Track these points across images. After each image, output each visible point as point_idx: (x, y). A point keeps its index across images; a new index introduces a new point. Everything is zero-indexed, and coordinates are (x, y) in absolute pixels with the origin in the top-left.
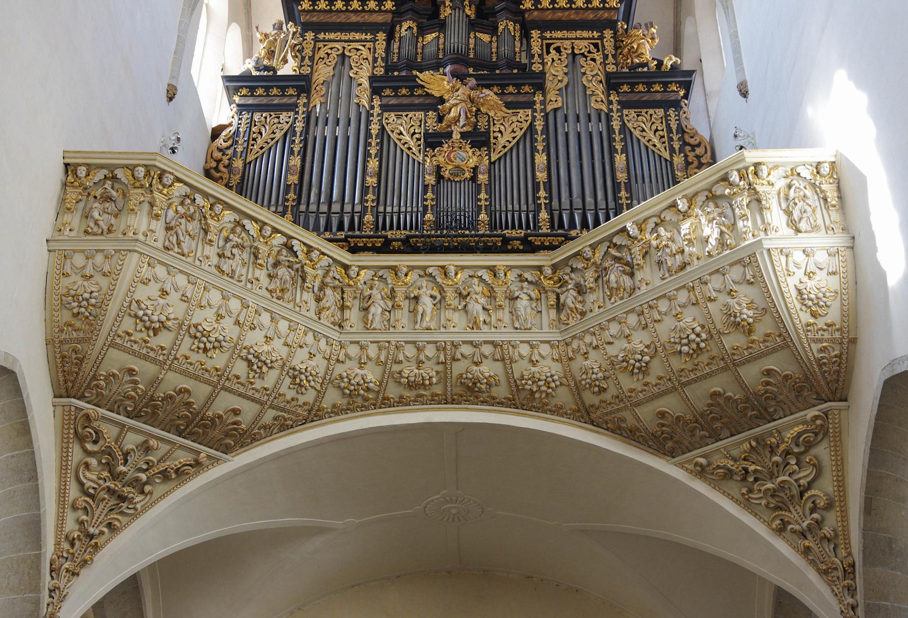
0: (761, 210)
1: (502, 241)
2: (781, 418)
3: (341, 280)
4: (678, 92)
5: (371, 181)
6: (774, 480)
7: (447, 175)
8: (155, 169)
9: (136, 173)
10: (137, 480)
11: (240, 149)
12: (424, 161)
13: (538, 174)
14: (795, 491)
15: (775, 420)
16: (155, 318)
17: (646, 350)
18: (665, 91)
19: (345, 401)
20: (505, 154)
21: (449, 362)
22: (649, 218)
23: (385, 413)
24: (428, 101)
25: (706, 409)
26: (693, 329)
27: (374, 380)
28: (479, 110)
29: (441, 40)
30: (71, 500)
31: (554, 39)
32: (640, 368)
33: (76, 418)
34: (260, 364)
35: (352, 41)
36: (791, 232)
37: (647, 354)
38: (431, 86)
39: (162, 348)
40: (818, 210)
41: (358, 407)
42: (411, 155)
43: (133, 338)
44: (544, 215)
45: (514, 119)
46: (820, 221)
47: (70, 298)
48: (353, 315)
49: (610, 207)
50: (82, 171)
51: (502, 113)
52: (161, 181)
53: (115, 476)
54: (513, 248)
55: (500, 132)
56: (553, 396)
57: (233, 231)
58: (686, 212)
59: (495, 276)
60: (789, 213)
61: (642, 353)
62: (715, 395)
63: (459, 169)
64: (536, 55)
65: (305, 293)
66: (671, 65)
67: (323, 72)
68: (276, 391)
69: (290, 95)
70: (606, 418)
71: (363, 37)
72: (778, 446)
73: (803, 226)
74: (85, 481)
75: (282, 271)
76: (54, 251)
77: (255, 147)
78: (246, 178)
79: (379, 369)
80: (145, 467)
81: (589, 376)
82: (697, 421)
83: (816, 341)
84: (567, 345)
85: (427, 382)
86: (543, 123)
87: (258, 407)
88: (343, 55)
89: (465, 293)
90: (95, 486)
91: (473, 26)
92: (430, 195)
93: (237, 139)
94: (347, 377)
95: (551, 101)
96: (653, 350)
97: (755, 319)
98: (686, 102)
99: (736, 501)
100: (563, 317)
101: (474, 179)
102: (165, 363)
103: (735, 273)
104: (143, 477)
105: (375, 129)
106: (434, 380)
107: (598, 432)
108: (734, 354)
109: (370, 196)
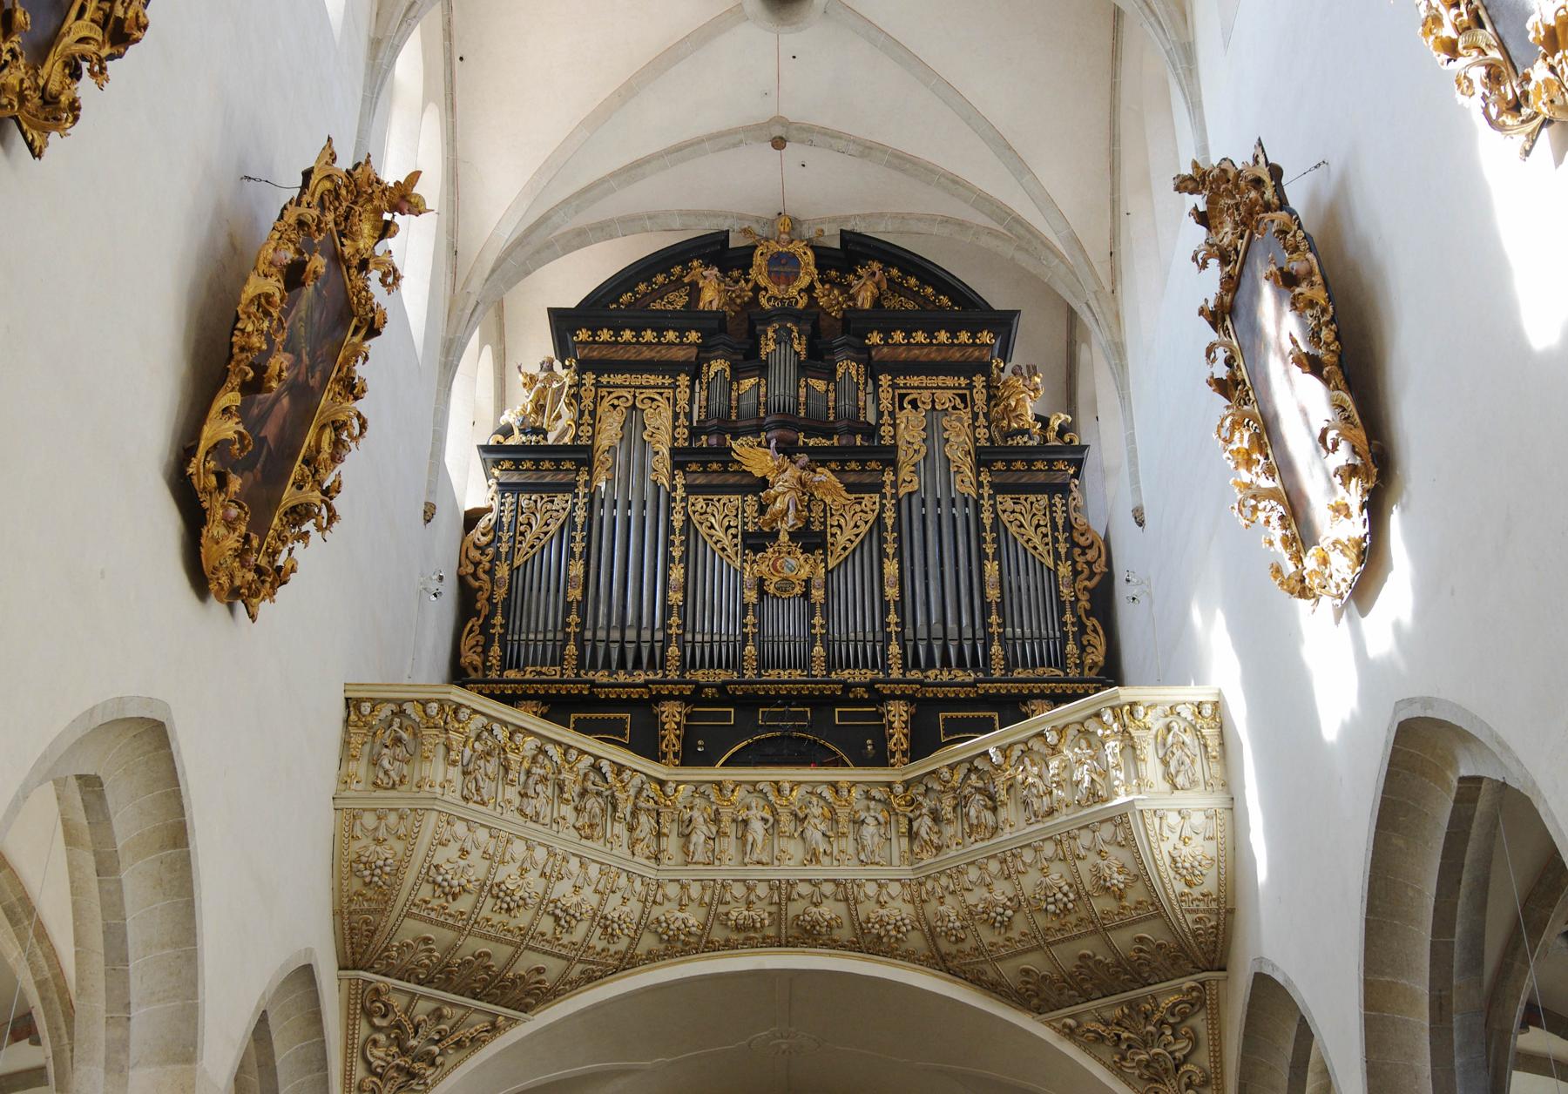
0: (1136, 759)
1: (842, 689)
2: (1156, 983)
3: (656, 798)
4: (1066, 470)
5: (676, 597)
6: (1148, 1049)
7: (771, 590)
8: (450, 703)
9: (429, 711)
10: (429, 1053)
11: (504, 549)
12: (743, 568)
13: (887, 589)
14: (1171, 1065)
15: (1150, 984)
16: (455, 882)
17: (1008, 903)
18: (1050, 470)
19: (662, 946)
20: (846, 558)
21: (783, 902)
22: (1015, 743)
23: (708, 958)
24: (745, 481)
25: (1074, 970)
26: (1060, 888)
27: (696, 924)
28: (812, 495)
29: (763, 390)
30: (357, 1082)
31: (909, 388)
32: (1002, 923)
33: (363, 992)
34: (568, 918)
35: (645, 387)
36: (1167, 786)
37: (1009, 908)
38: (751, 463)
39: (462, 913)
40: (1198, 758)
41: (677, 952)
42: (725, 558)
43: (429, 906)
44: (894, 649)
45: (858, 508)
46: (1199, 775)
47: (362, 866)
48: (672, 844)
49: (977, 637)
50: (366, 708)
51: (842, 499)
52: (456, 716)
53: (404, 1051)
54: (856, 696)
55: (839, 526)
56: (903, 941)
57: (534, 760)
58: (1056, 745)
59: (837, 792)
60: (1165, 763)
61: (1005, 907)
62: (1083, 957)
63: (786, 584)
64: (886, 412)
65: (616, 824)
66: (1060, 425)
67: (610, 431)
68: (585, 944)
69: (566, 470)
70: (964, 968)
71: (660, 381)
72: (1153, 1013)
73: (1180, 780)
74: (372, 1059)
75: (593, 804)
76: (342, 809)
77: (524, 545)
78: (514, 590)
79: (703, 911)
80: (437, 1037)
81: (945, 923)
82: (1065, 981)
83: (1191, 911)
84: (920, 884)
85: (758, 925)
86: (894, 515)
87: (565, 963)
88: (634, 407)
89: (801, 815)
90: (383, 1064)
91: (803, 369)
92: (750, 619)
93: (500, 533)
94: (665, 921)
95: (904, 481)
96: (1017, 903)
97: (1126, 885)
98: (1077, 482)
99: (1108, 1067)
100: (916, 849)
101: (806, 595)
102: (464, 929)
103: (1106, 831)
104: (436, 1049)
105: (678, 520)
106: (767, 922)
107: (955, 982)
108: (1104, 919)
109: (675, 620)
